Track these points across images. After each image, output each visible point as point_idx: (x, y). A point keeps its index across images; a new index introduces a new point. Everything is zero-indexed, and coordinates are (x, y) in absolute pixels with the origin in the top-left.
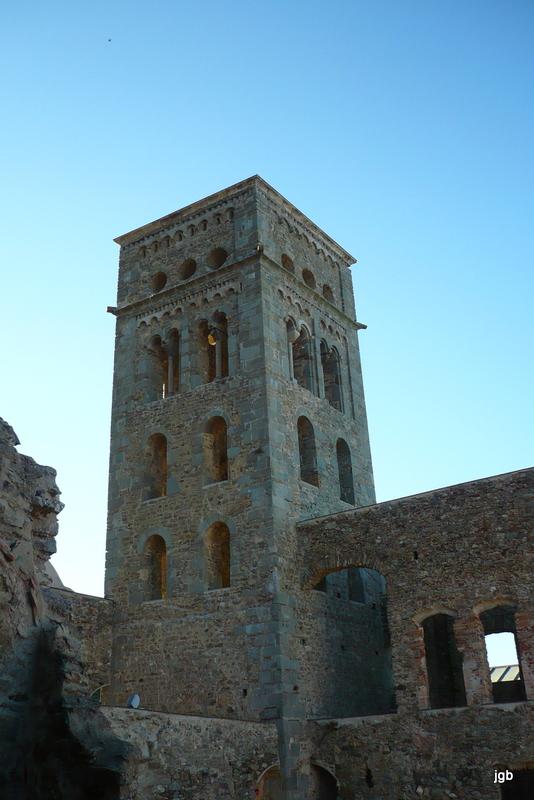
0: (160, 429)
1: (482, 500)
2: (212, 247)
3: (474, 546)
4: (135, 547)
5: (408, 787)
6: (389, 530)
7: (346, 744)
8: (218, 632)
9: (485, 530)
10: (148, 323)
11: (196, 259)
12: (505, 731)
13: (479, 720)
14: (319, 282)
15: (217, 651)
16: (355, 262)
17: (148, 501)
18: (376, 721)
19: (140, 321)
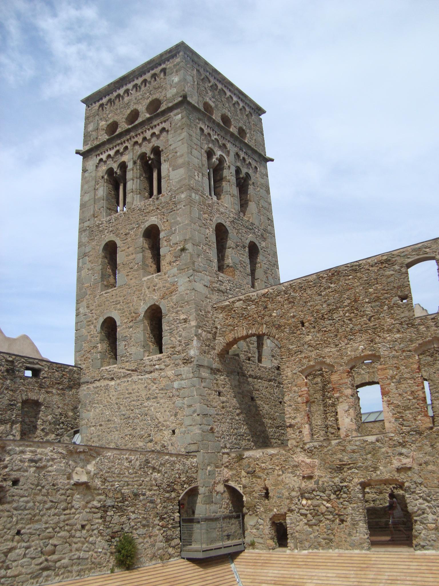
0: (112, 237)
1: (354, 278)
2: (150, 99)
3: (347, 314)
4: (95, 327)
6: (282, 305)
7: (250, 469)
8: (154, 388)
9: (356, 301)
10: (104, 159)
11: (139, 109)
12: (369, 456)
13: (349, 448)
15: (154, 402)
16: (264, 112)
17: (104, 292)
19: (99, 158)
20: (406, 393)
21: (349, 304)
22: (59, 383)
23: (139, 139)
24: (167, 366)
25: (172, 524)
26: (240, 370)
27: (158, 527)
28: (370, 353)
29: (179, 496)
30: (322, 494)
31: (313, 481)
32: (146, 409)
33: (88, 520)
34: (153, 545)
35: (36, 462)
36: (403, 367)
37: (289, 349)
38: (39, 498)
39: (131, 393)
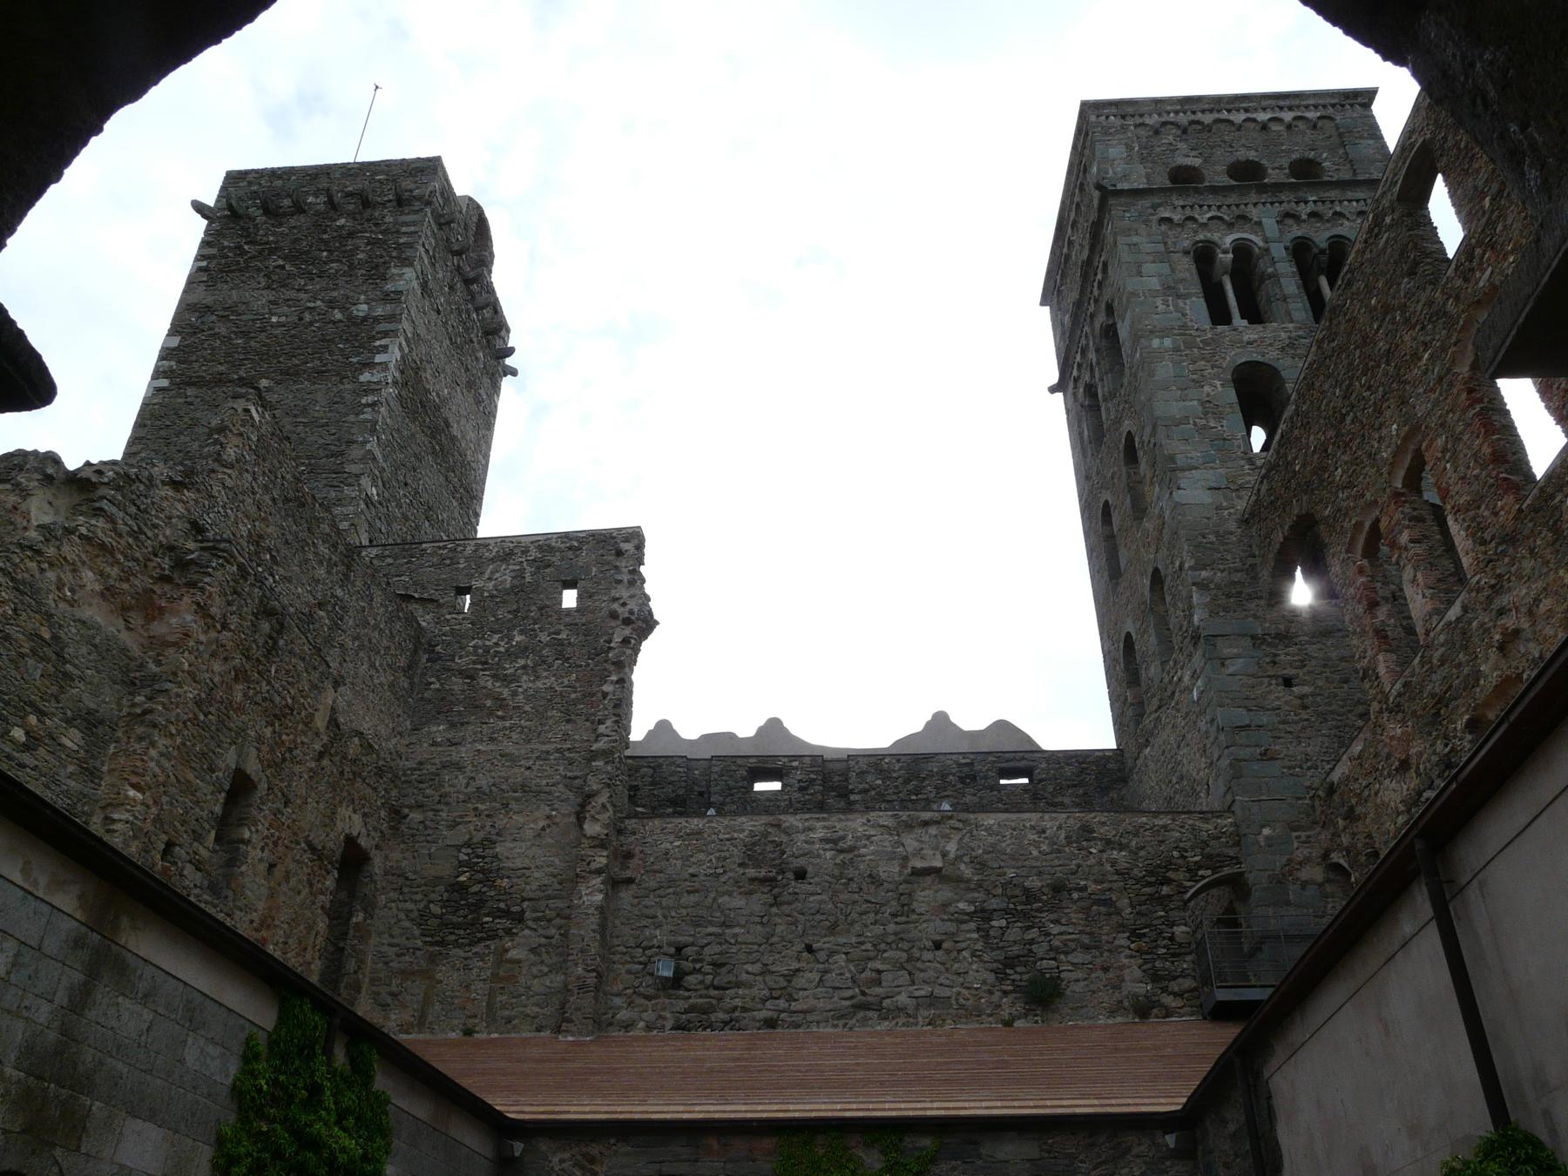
12: (1461, 655)
20: (1469, 468)
21: (1359, 357)
27: (1127, 952)
28: (1407, 428)
29: (1185, 893)
33: (946, 933)
34: (1116, 987)
35: (835, 842)
36: (1451, 415)
38: (843, 897)
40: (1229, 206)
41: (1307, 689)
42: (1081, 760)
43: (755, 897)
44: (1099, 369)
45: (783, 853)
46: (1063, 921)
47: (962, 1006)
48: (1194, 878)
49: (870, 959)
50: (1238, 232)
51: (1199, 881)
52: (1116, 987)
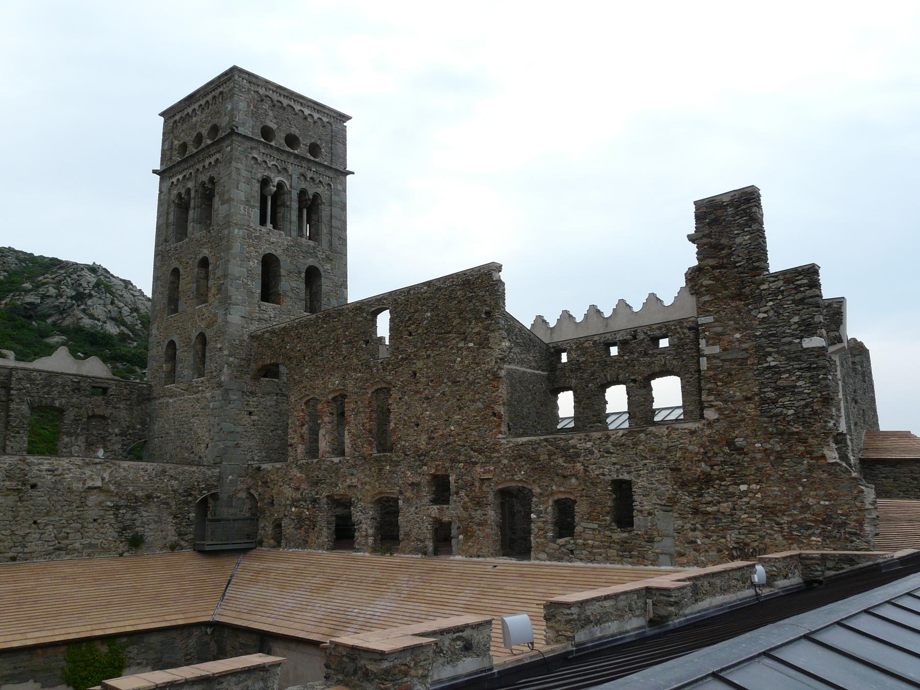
1: (338, 321)
3: (331, 353)
4: (162, 348)
5: (288, 508)
7: (264, 480)
8: (197, 407)
9: (337, 342)
11: (203, 133)
12: (333, 474)
13: (323, 466)
14: (304, 143)
16: (349, 118)
18: (278, 466)
19: (171, 181)
22: (126, 400)
23: (200, 166)
24: (207, 388)
25: (186, 522)
26: (279, 391)
27: (172, 524)
30: (304, 503)
31: (300, 492)
32: (192, 424)
34: (165, 539)
35: (53, 471)
37: (294, 379)
38: (55, 498)
39: (182, 410)
40: (281, 161)
41: (256, 418)
42: (132, 387)
43: (11, 497)
44: (195, 202)
45: (26, 475)
46: (149, 511)
47: (103, 548)
48: (201, 494)
49: (64, 527)
50: (284, 177)
51: (202, 496)
52: (165, 539)
